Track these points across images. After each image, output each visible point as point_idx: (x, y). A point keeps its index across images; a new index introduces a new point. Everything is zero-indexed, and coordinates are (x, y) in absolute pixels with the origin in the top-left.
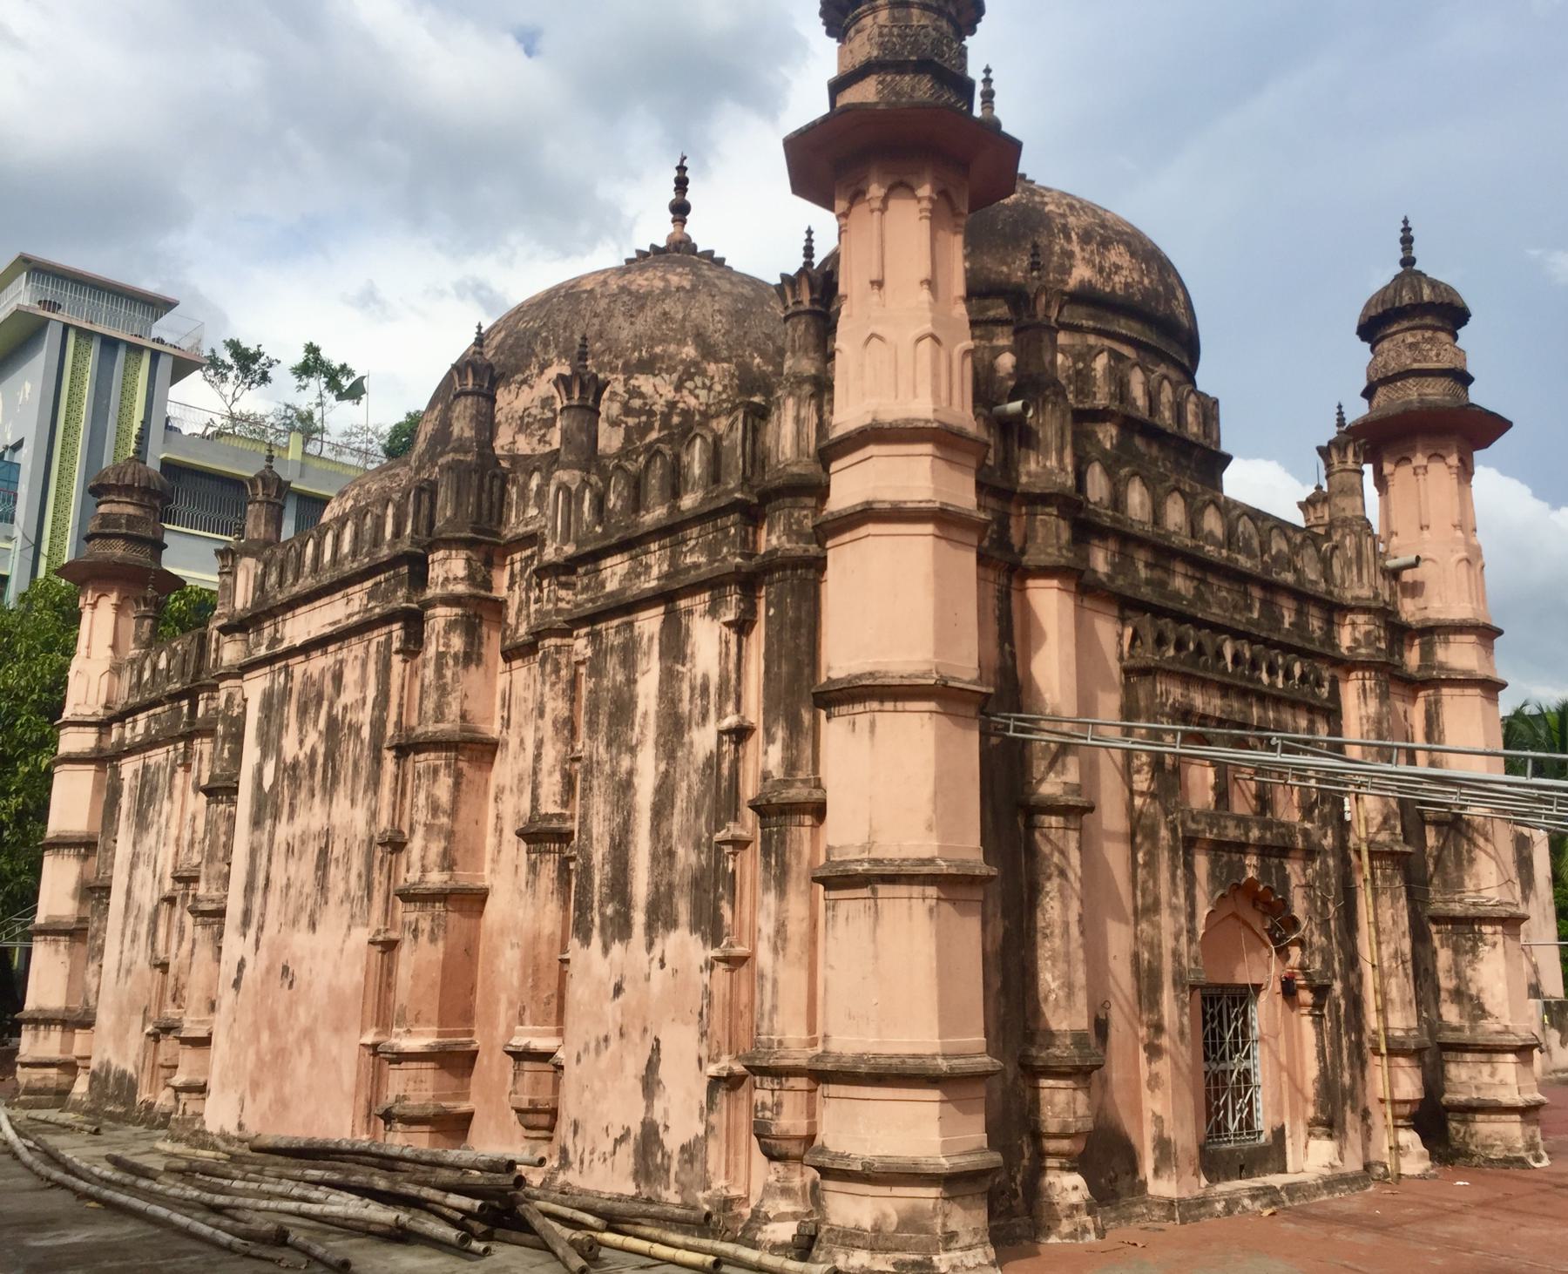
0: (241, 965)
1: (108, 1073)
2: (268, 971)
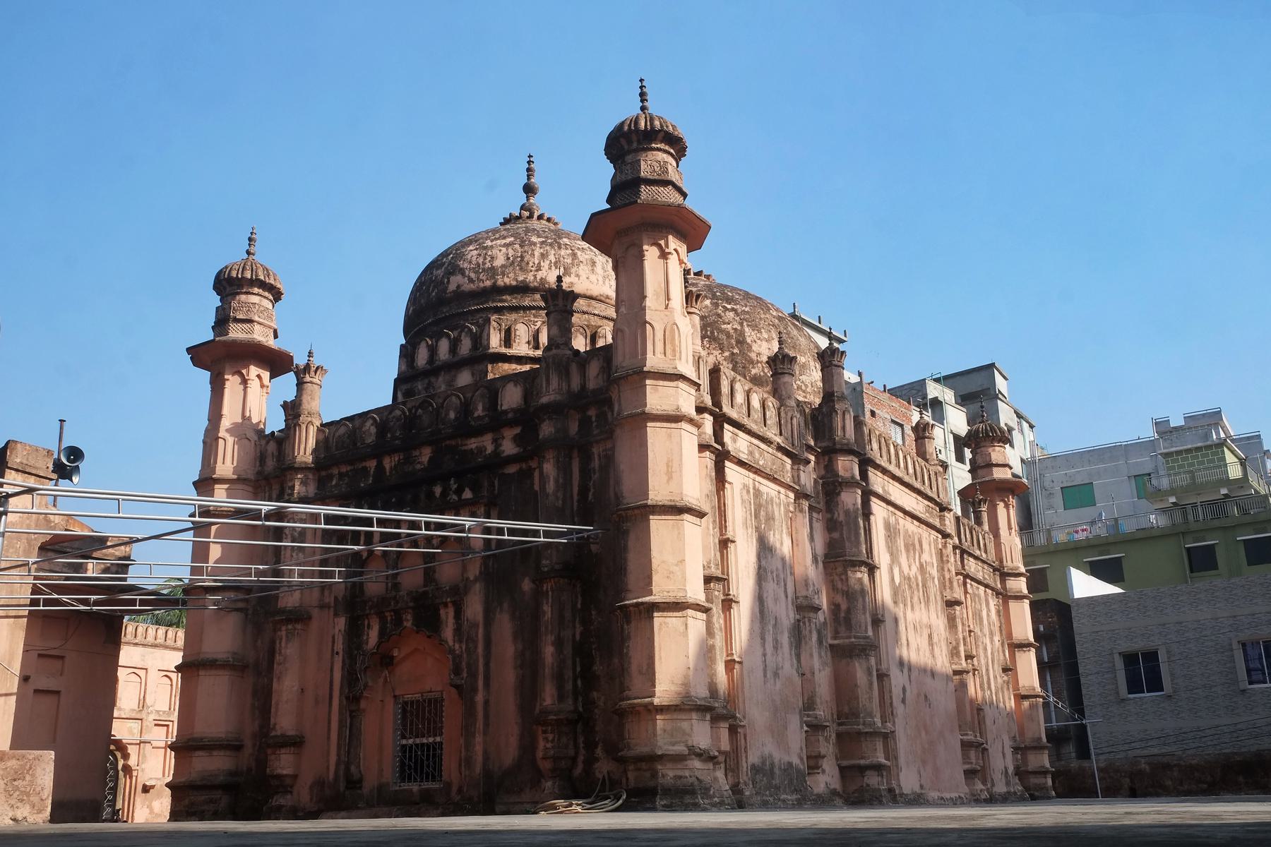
0: (904, 689)
1: (772, 764)
2: (919, 695)
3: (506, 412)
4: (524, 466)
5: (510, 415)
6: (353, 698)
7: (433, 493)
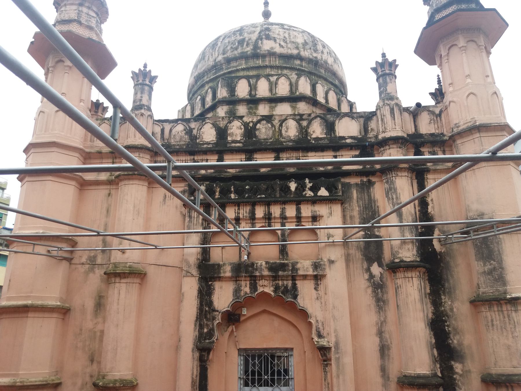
3: (343, 138)
4: (365, 179)
5: (349, 141)
6: (204, 350)
7: (289, 188)
